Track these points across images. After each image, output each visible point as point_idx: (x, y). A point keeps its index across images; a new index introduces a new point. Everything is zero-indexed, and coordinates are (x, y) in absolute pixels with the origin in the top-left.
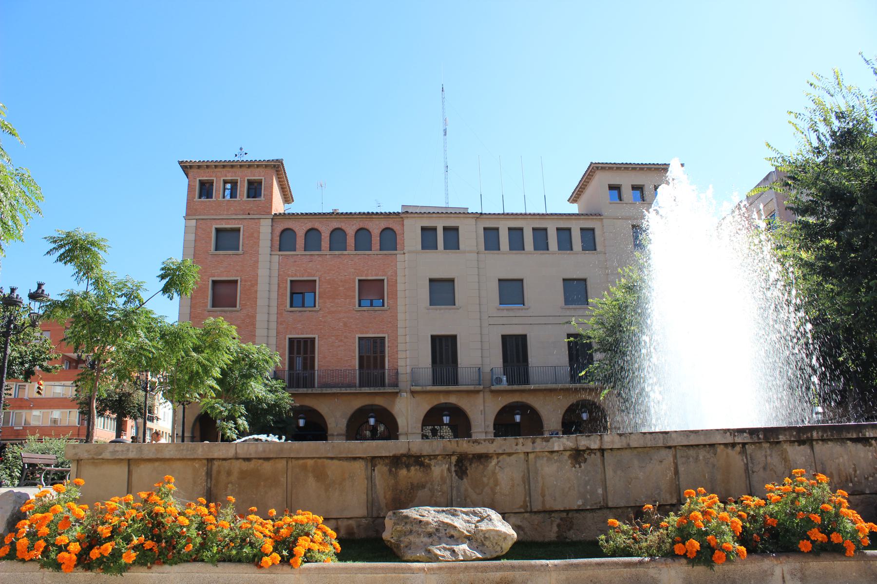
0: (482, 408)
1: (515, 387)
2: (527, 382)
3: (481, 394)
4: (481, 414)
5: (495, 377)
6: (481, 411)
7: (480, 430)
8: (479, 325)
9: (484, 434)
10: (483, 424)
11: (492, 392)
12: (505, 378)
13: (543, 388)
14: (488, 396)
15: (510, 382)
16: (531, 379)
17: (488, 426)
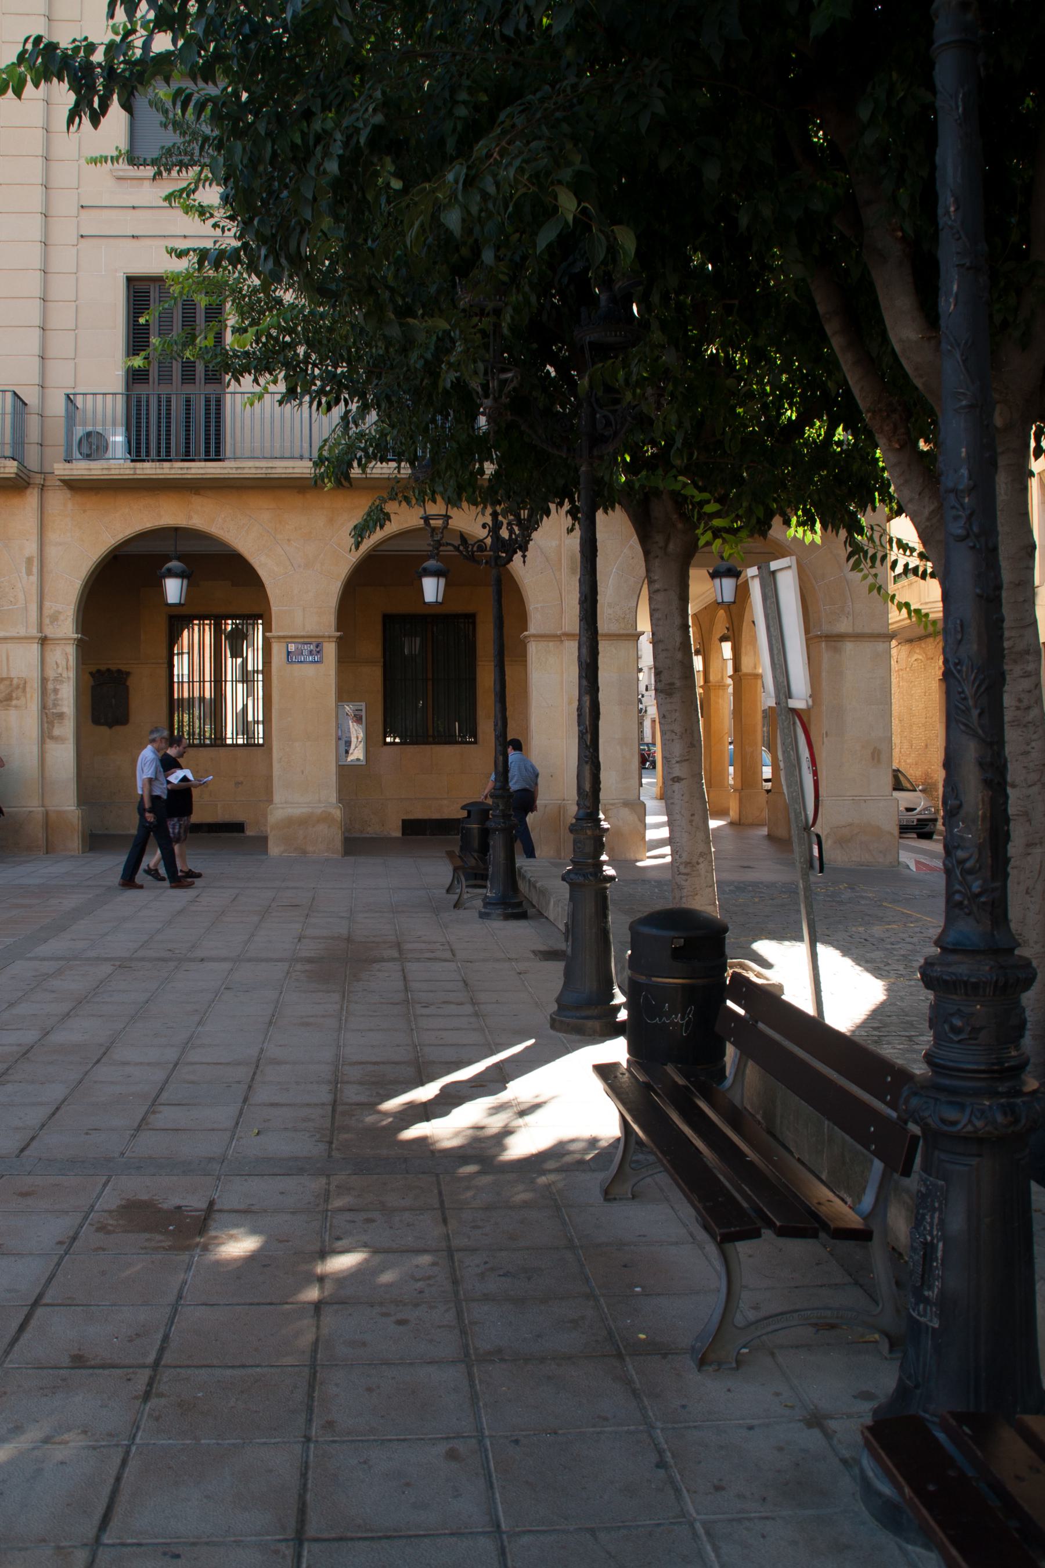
0: (31, 548)
1: (148, 469)
2: (214, 451)
3: (32, 498)
4: (29, 573)
5: (79, 431)
6: (29, 561)
7: (22, 632)
8: (38, 235)
9: (35, 648)
10: (33, 608)
11: (76, 486)
12: (118, 438)
13: (260, 473)
14: (59, 501)
15: (137, 451)
16: (228, 449)
17: (55, 618)
